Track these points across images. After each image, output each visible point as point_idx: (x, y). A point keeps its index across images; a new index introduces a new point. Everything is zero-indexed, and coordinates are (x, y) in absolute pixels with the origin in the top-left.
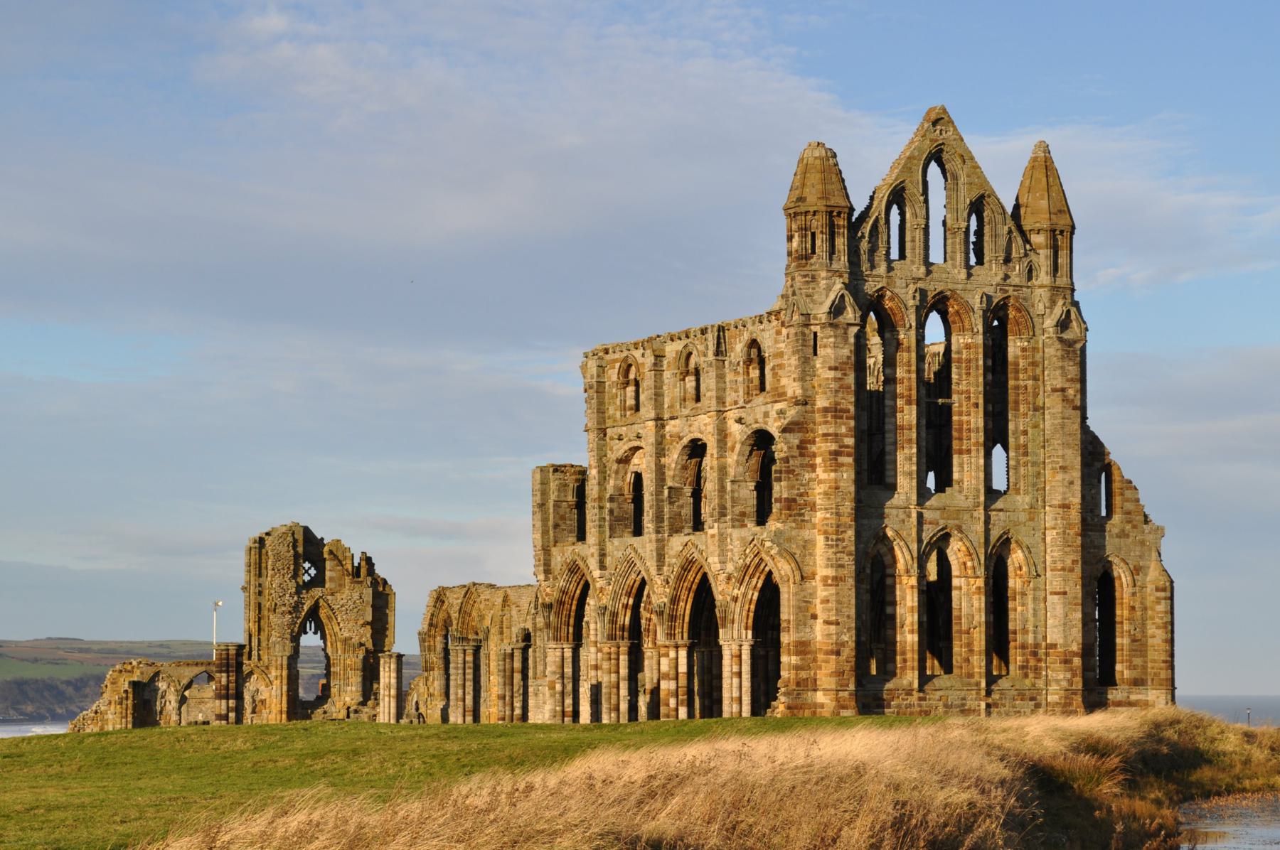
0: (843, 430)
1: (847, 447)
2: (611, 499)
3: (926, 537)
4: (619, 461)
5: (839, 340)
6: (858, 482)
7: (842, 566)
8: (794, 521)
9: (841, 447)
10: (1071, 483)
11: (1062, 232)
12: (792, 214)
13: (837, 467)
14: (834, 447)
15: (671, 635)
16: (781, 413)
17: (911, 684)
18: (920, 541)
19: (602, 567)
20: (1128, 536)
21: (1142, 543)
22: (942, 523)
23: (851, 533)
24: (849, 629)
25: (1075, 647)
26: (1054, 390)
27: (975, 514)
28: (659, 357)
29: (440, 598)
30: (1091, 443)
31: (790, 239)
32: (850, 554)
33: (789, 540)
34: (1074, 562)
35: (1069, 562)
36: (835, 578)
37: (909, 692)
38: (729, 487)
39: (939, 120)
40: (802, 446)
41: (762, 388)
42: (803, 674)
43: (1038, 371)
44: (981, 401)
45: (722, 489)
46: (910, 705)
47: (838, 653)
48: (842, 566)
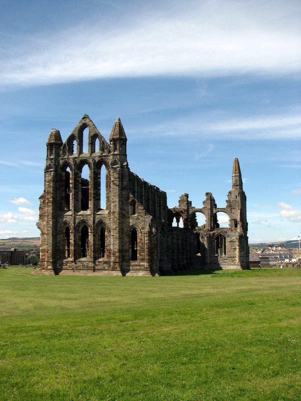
0: (49, 197)
1: (50, 201)
3: (77, 222)
5: (49, 175)
6: (53, 209)
7: (49, 231)
8: (42, 220)
9: (49, 201)
10: (116, 206)
11: (117, 140)
12: (47, 146)
13: (48, 206)
18: (74, 223)
20: (139, 219)
21: (144, 221)
22: (82, 218)
23: (51, 222)
25: (116, 250)
27: (92, 216)
34: (116, 227)
35: (115, 227)
37: (72, 262)
46: (73, 265)
47: (47, 252)
48: (49, 231)
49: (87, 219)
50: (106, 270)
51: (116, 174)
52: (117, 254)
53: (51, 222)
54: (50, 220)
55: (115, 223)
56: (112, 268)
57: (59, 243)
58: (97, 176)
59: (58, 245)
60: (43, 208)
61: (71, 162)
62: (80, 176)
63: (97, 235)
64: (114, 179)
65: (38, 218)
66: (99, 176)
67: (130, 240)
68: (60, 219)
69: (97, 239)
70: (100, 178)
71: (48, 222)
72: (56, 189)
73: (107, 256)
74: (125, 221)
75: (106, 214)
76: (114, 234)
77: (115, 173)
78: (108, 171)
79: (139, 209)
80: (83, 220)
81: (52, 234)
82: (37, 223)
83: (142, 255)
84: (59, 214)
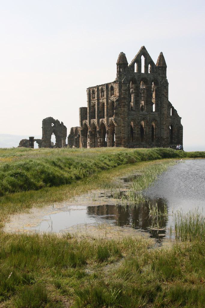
2: (91, 113)
4: (92, 106)
10: (165, 110)
15: (99, 135)
16: (116, 98)
19: (90, 124)
20: (175, 119)
21: (178, 120)
28: (98, 89)
29: (72, 129)
31: (117, 69)
36: (124, 126)
38: (108, 111)
39: (144, 49)
40: (119, 104)
41: (113, 94)
42: (119, 142)
45: (107, 111)
52: (165, 140)
61: (136, 77)
68: (130, 117)
78: (157, 87)
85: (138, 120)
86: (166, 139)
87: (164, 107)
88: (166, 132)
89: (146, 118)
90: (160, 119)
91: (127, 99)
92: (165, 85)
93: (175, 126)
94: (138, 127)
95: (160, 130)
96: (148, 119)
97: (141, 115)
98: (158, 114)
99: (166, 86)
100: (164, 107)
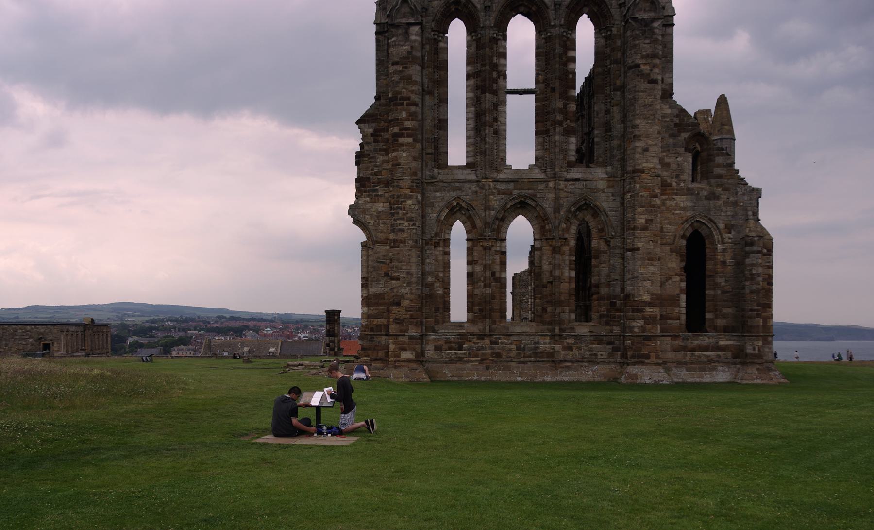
0: (404, 114)
7: (403, 231)
8: (368, 196)
9: (401, 130)
10: (646, 150)
14: (396, 130)
17: (485, 329)
20: (717, 198)
21: (735, 204)
22: (515, 192)
24: (409, 284)
26: (631, 68)
30: (677, 116)
32: (410, 220)
33: (364, 211)
34: (647, 221)
35: (641, 221)
36: (395, 241)
42: (377, 322)
43: (619, 55)
44: (557, 84)
48: (403, 231)
49: (535, 196)
50: (598, 363)
51: (647, 41)
52: (648, 309)
53: (409, 202)
54: (406, 194)
55: (643, 207)
56: (633, 357)
57: (430, 274)
58: (566, 53)
59: (429, 279)
60: (372, 155)
62: (501, 50)
63: (566, 249)
64: (643, 57)
65: (354, 190)
66: (570, 54)
67: (683, 264)
68: (438, 194)
69: (567, 262)
70: (573, 60)
71: (395, 204)
72: (423, 90)
73: (601, 316)
74: (668, 203)
75: (602, 179)
76: (640, 245)
77: (646, 38)
78: (606, 38)
79: (718, 166)
80: (519, 196)
81: (416, 242)
82: (353, 210)
83: (724, 316)
84: (432, 177)
85: (487, 208)
86: (650, 304)
87: (634, 136)
88: (652, 269)
89: (532, 197)
90: (622, 204)
91: (415, 104)
92: (640, 18)
93: (717, 237)
94: (486, 244)
95: (623, 258)
96: (548, 206)
97: (502, 187)
98: (611, 176)
99: (653, 20)
100: (637, 133)
